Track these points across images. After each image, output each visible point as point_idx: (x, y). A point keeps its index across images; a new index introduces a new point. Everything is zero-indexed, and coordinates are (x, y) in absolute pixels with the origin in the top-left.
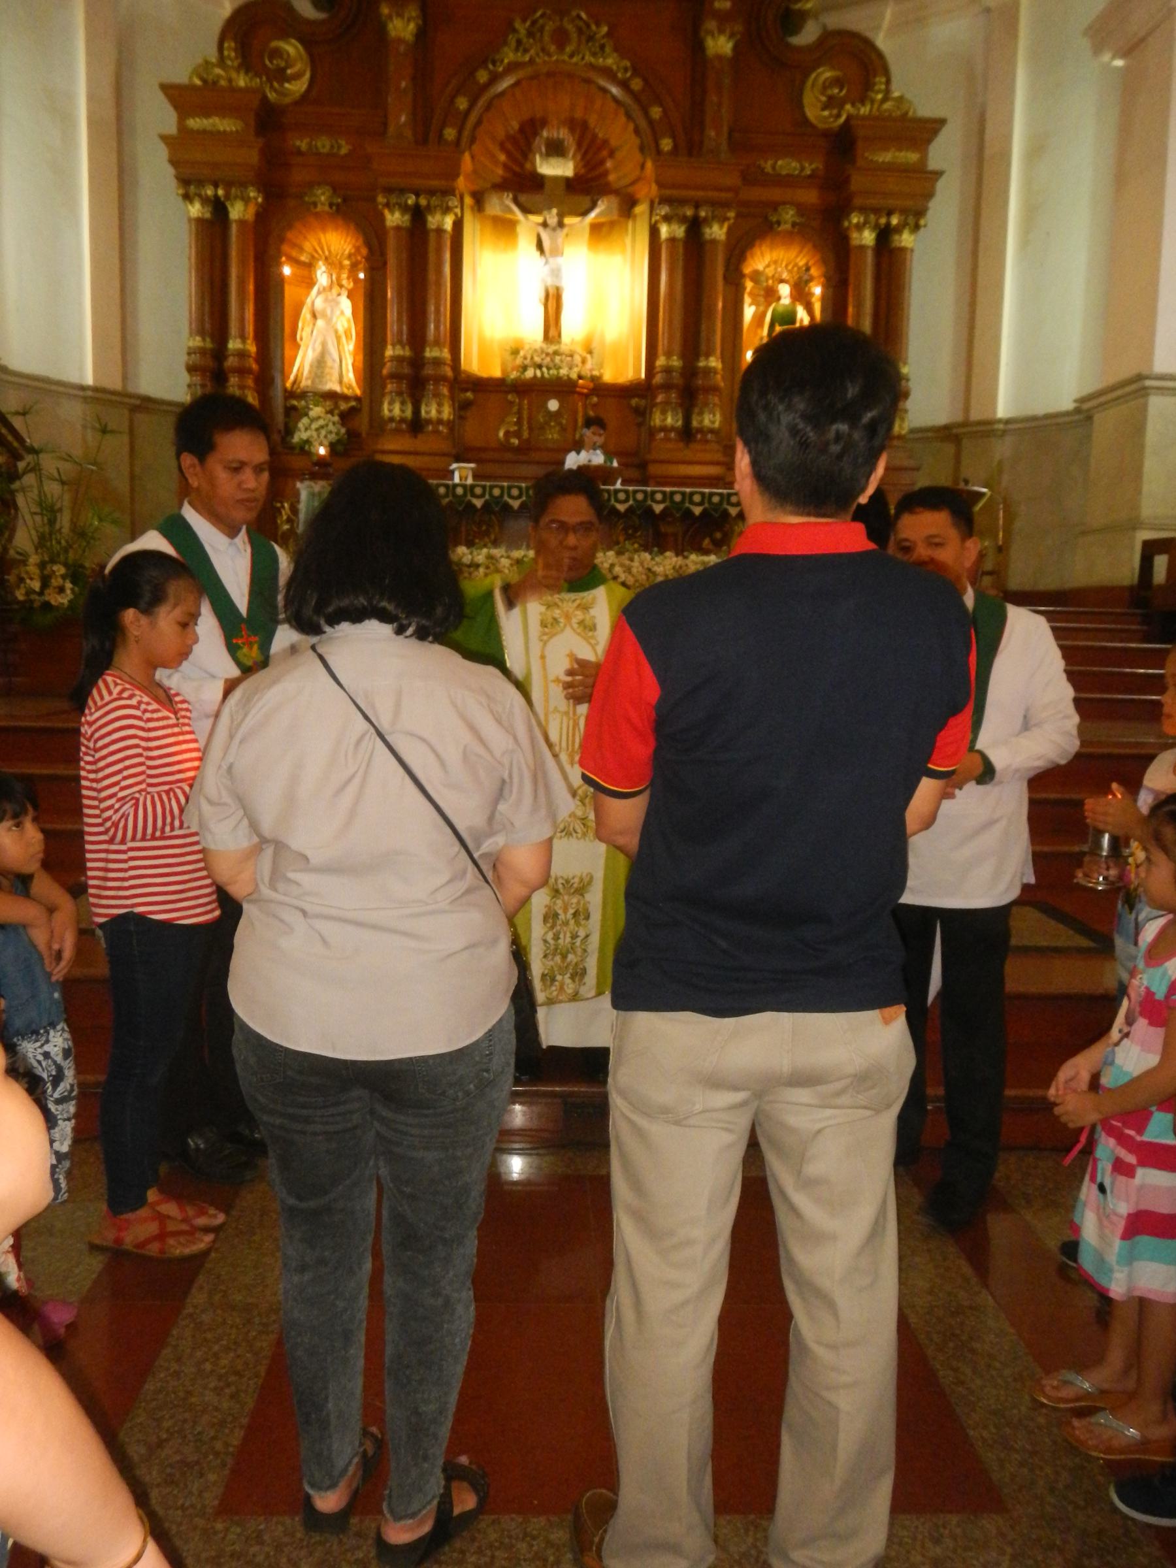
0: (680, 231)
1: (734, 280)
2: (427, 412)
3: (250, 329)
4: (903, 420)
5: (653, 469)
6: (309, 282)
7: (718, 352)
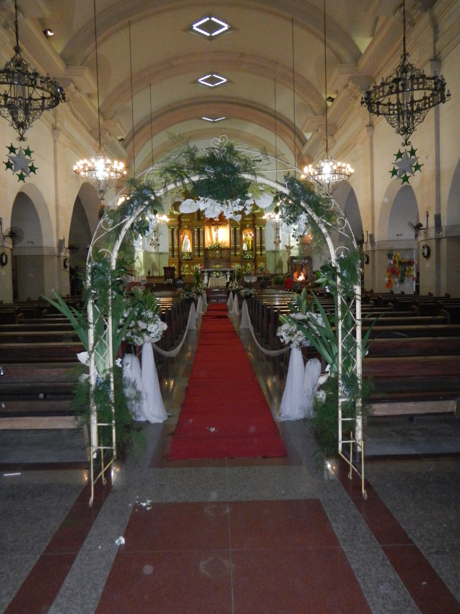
0: (233, 229)
1: (241, 234)
3: (177, 244)
6: (184, 237)
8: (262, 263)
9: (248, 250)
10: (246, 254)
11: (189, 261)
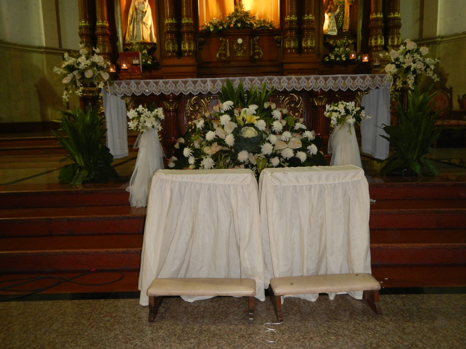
2: (184, 47)
4: (398, 38)
5: (286, 67)
7: (313, 11)
10: (331, 49)
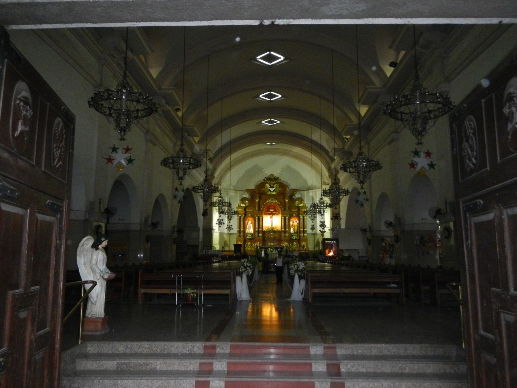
0: (284, 217)
6: (248, 223)
8: (304, 243)
9: (294, 233)
10: (292, 236)
11: (251, 240)
